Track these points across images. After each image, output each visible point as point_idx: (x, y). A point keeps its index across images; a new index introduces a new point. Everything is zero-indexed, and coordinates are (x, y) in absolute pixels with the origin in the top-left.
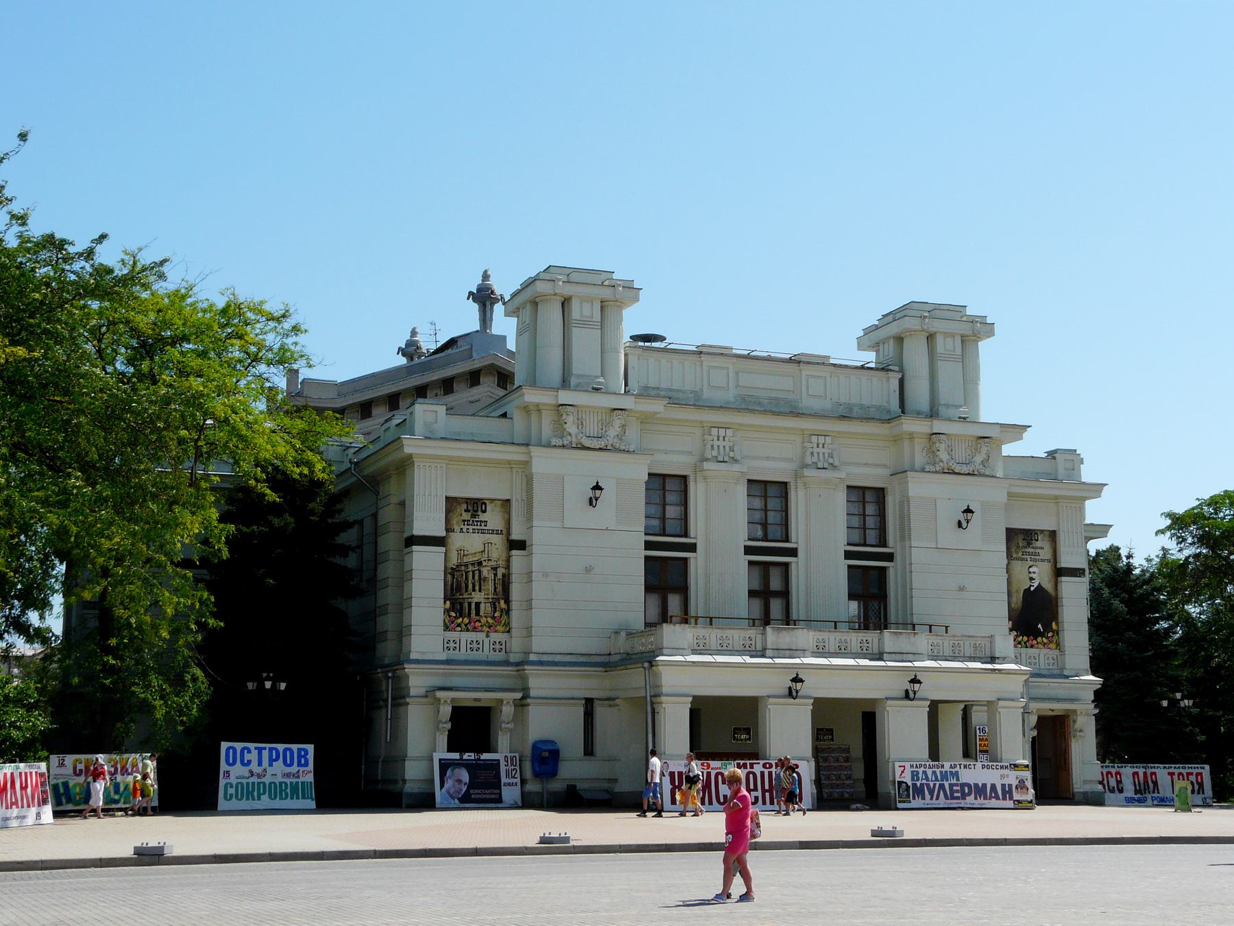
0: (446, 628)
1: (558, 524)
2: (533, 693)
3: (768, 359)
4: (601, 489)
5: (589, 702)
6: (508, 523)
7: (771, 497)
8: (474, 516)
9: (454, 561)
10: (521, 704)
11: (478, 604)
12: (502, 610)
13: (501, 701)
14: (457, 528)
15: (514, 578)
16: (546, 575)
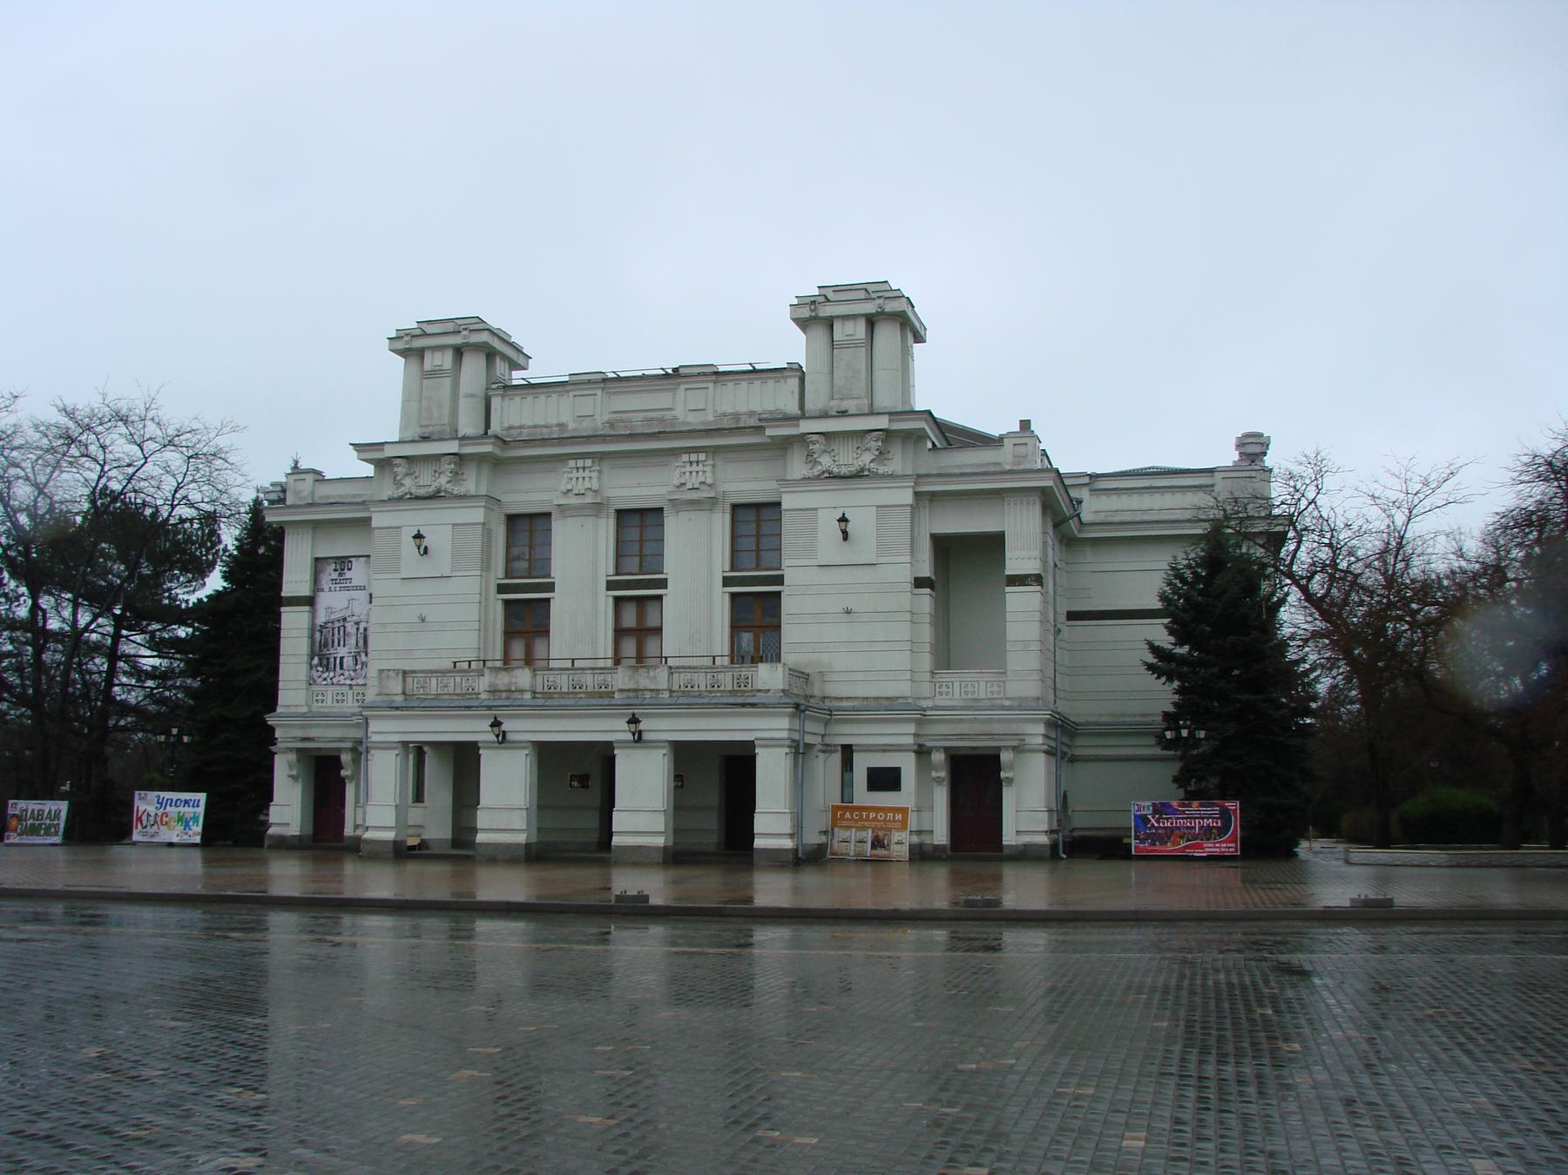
3: (643, 377)
7: (639, 527)
9: (321, 619)
13: (340, 750)
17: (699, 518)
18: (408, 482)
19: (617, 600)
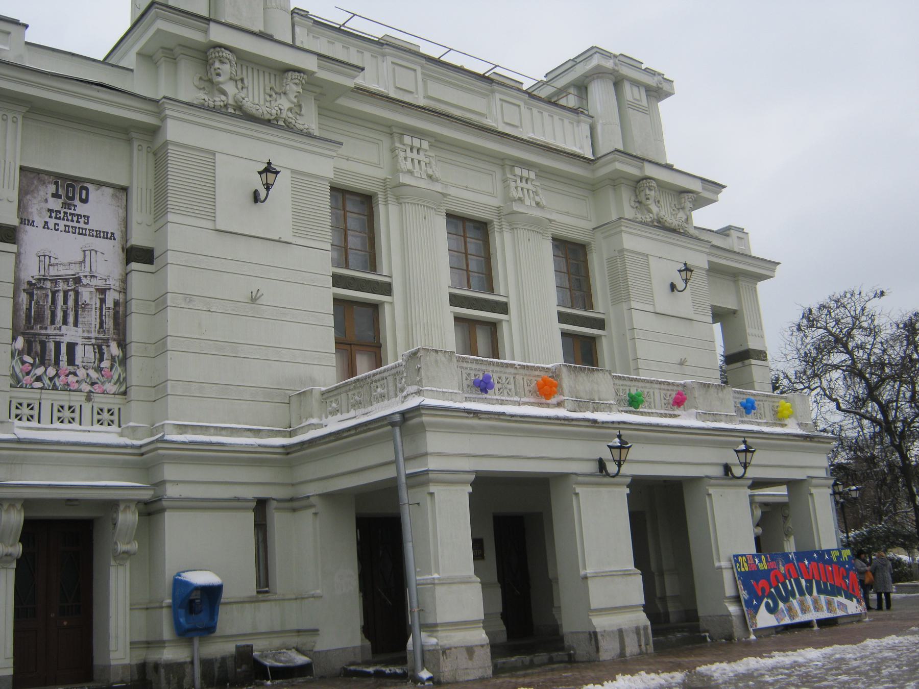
0: (17, 382)
1: (210, 225)
2: (172, 491)
5: (261, 505)
6: (126, 223)
8: (65, 205)
9: (31, 271)
10: (151, 510)
11: (71, 347)
12: (113, 358)
13: (111, 506)
14: (39, 222)
15: (134, 306)
16: (188, 298)
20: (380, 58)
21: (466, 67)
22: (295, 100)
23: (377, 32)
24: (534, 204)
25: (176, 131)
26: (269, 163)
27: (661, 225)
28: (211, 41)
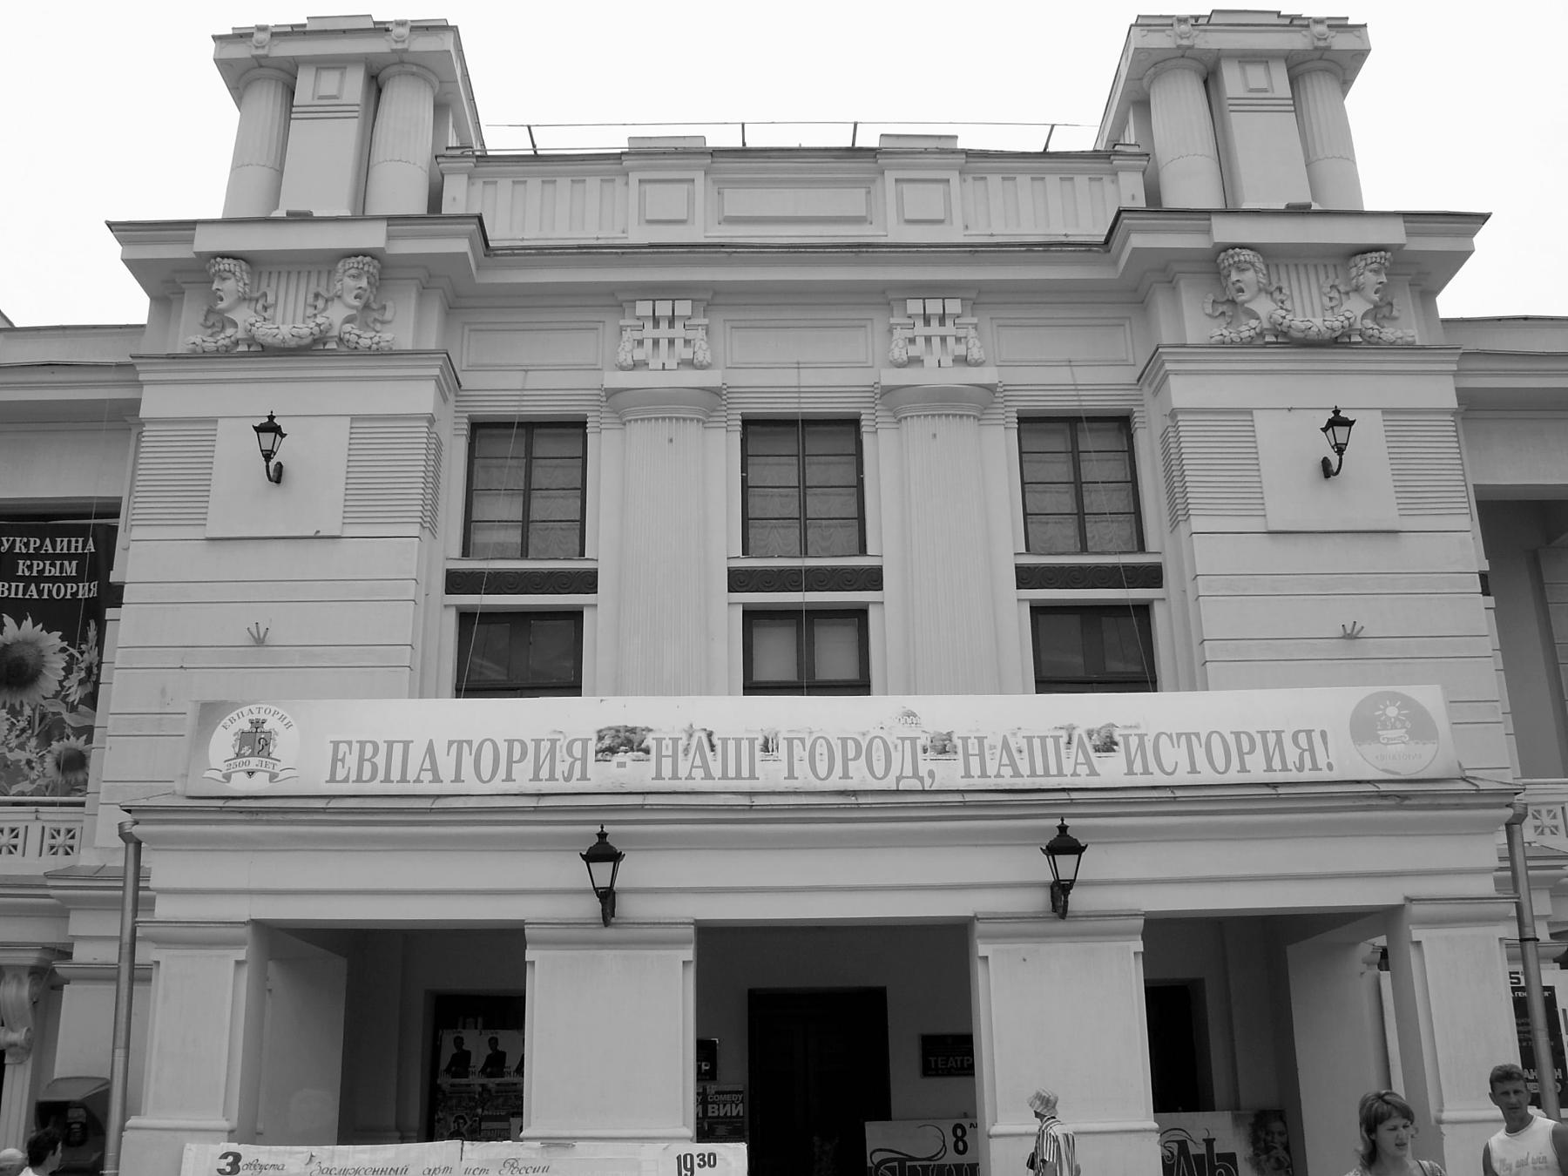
2: (81, 954)
4: (277, 430)
7: (807, 453)
17: (956, 434)
18: (244, 316)
19: (753, 617)
20: (619, 181)
21: (804, 145)
22: (357, 303)
23: (615, 141)
24: (947, 361)
25: (155, 402)
26: (271, 418)
27: (1287, 340)
28: (199, 254)
